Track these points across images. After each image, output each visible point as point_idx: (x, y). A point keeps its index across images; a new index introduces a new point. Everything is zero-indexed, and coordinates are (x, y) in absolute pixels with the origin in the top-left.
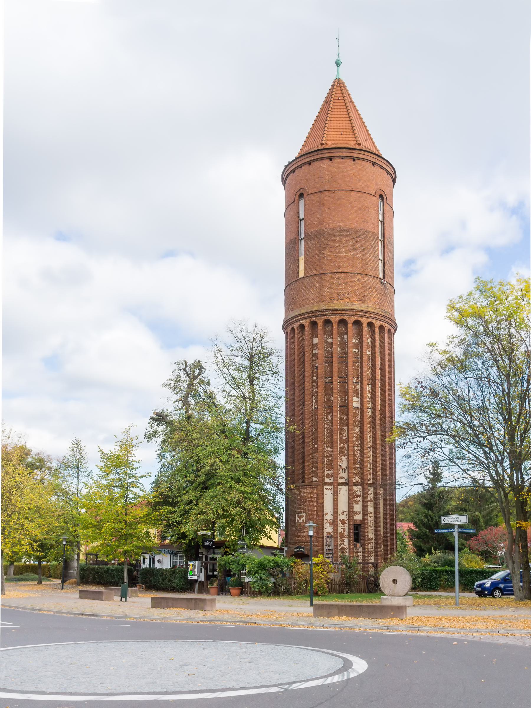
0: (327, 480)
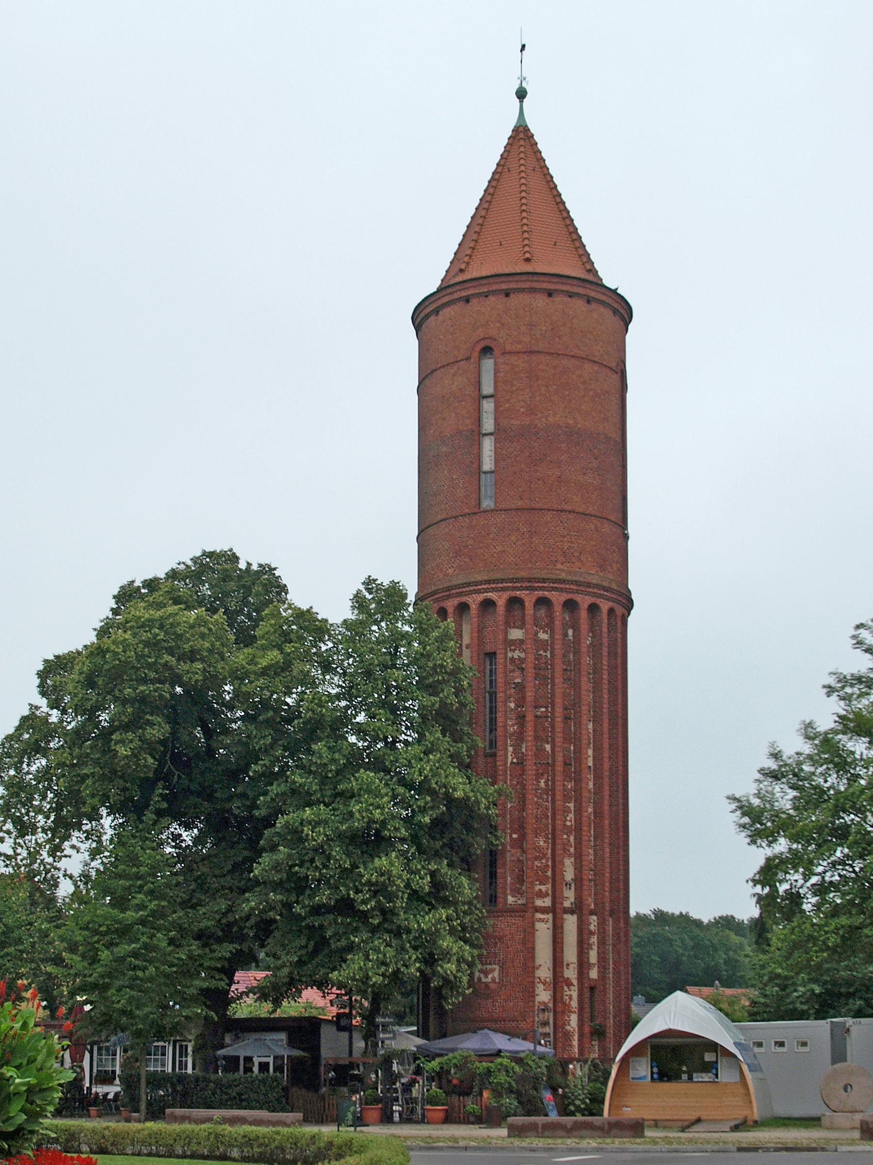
0: (539, 903)
